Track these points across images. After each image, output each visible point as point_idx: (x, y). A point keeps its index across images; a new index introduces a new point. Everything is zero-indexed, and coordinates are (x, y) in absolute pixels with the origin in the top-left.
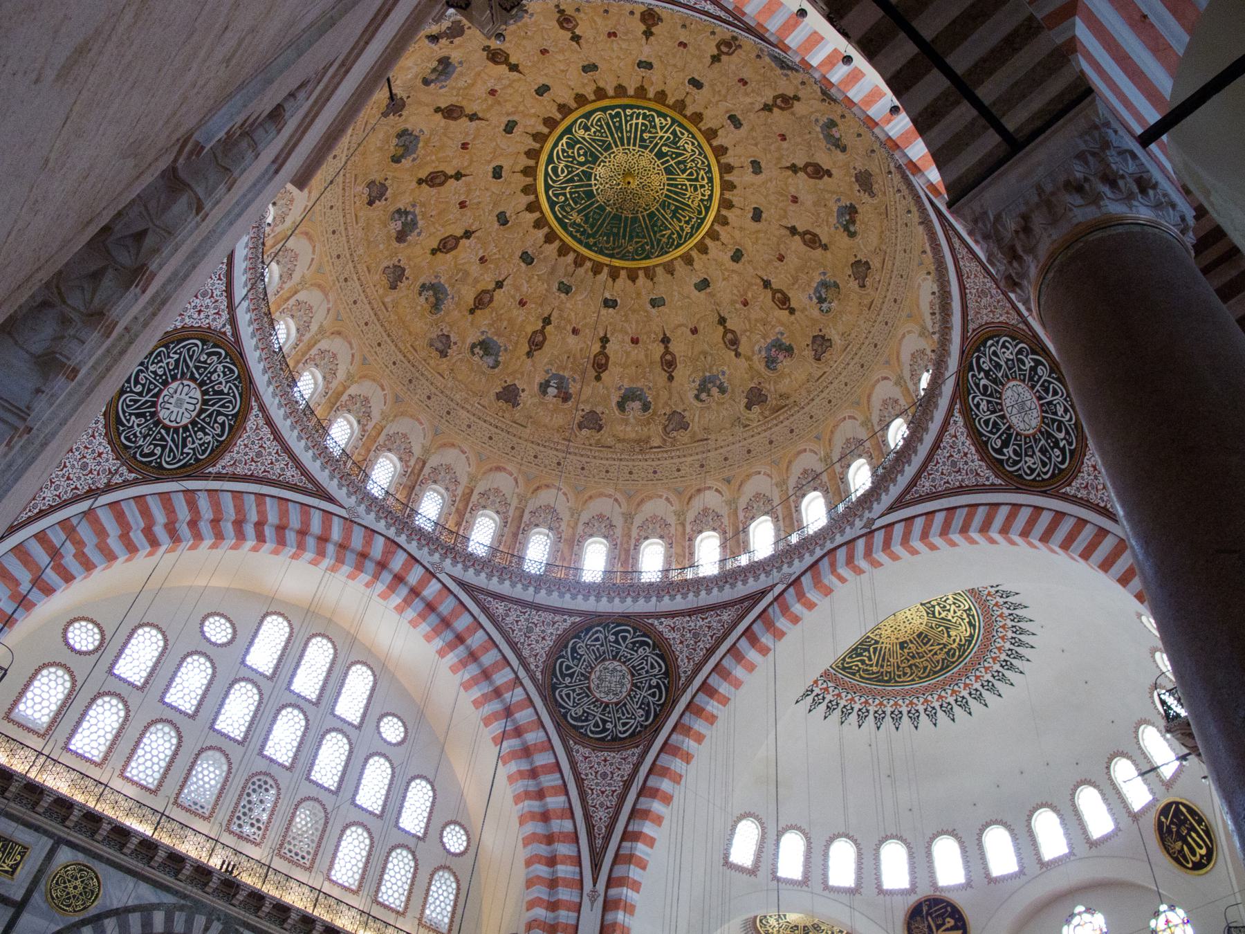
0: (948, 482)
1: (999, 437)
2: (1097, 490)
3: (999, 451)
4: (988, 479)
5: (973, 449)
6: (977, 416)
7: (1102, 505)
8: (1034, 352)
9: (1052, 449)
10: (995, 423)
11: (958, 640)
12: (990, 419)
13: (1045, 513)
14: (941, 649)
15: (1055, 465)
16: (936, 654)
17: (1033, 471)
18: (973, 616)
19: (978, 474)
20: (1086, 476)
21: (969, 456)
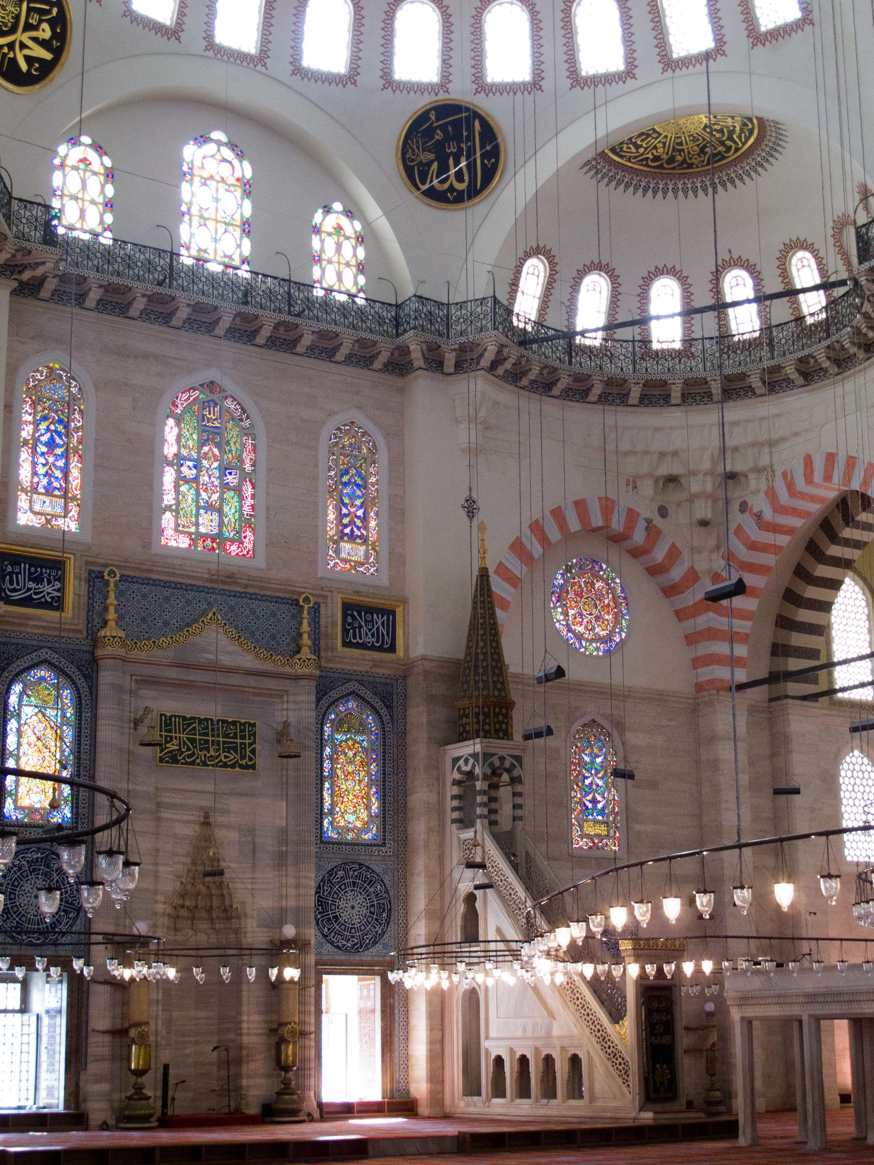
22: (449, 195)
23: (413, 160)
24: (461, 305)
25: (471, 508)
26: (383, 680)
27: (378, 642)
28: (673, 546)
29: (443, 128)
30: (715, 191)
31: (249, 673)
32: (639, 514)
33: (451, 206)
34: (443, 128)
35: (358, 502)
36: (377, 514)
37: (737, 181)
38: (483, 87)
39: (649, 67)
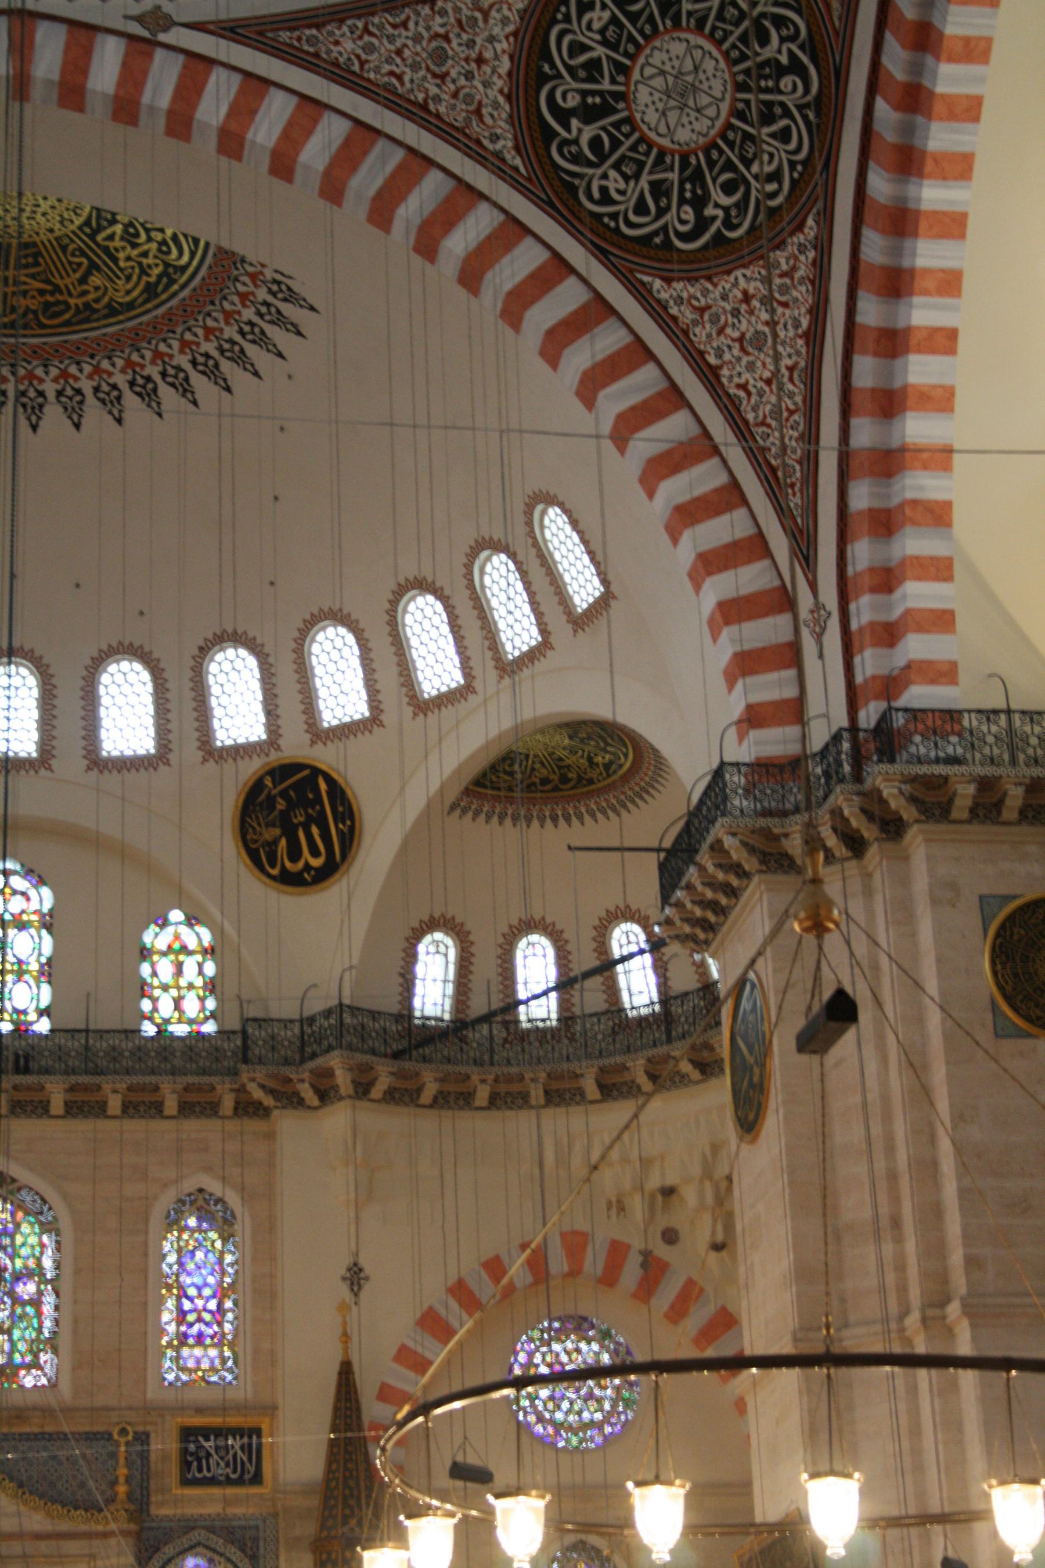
0: (399, 77)
1: (584, 94)
2: (721, 331)
3: (563, 116)
4: (495, 138)
5: (505, 65)
6: (567, 19)
7: (712, 360)
8: (812, 47)
9: (682, 201)
10: (594, 66)
11: (91, 296)
12: (591, 49)
13: (572, 281)
14: (42, 292)
15: (665, 228)
16: (25, 293)
17: (606, 198)
18: (174, 281)
19: (478, 112)
20: (717, 292)
21: (487, 69)
22: (306, 875)
23: (256, 841)
24: (311, 1020)
25: (355, 1277)
26: (243, 1523)
27: (235, 1471)
28: (690, 1283)
29: (283, 794)
30: (619, 815)
31: (39, 1537)
32: (628, 1247)
33: (308, 889)
34: (283, 794)
35: (207, 1292)
36: (235, 1303)
37: (574, 819)
38: (318, 734)
39: (487, 676)
